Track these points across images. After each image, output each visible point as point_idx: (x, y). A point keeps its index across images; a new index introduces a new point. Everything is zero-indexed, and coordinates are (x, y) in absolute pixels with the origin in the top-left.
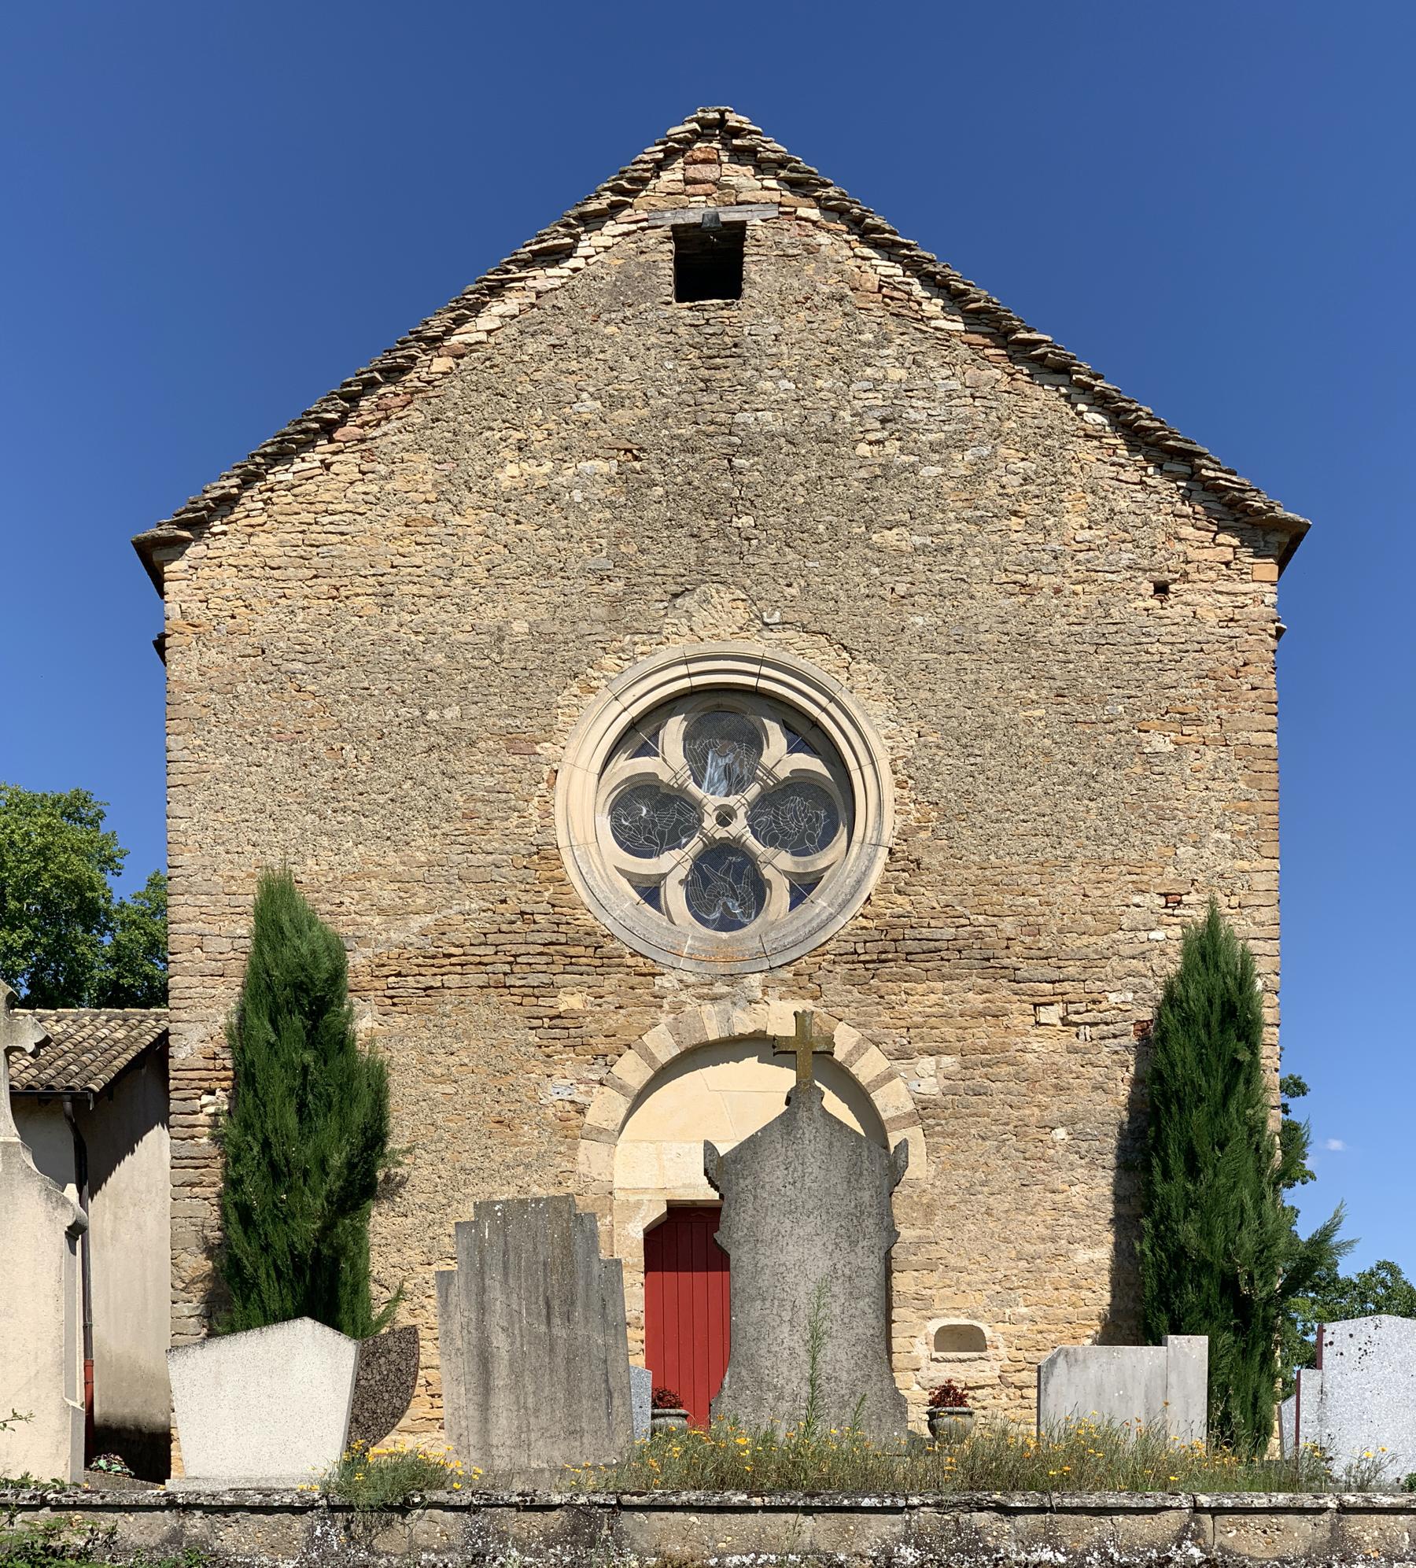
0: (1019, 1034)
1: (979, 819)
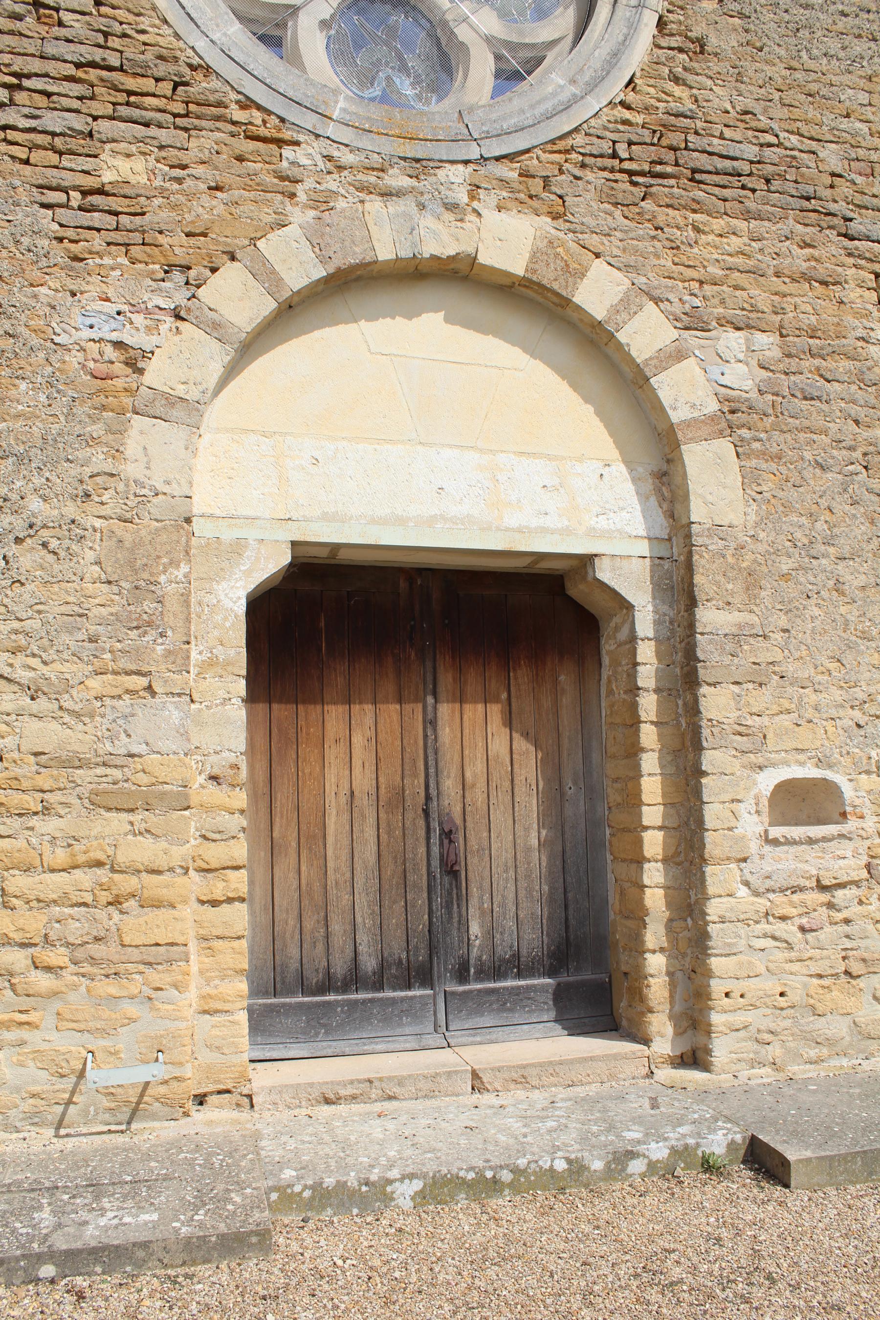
0: (858, 315)
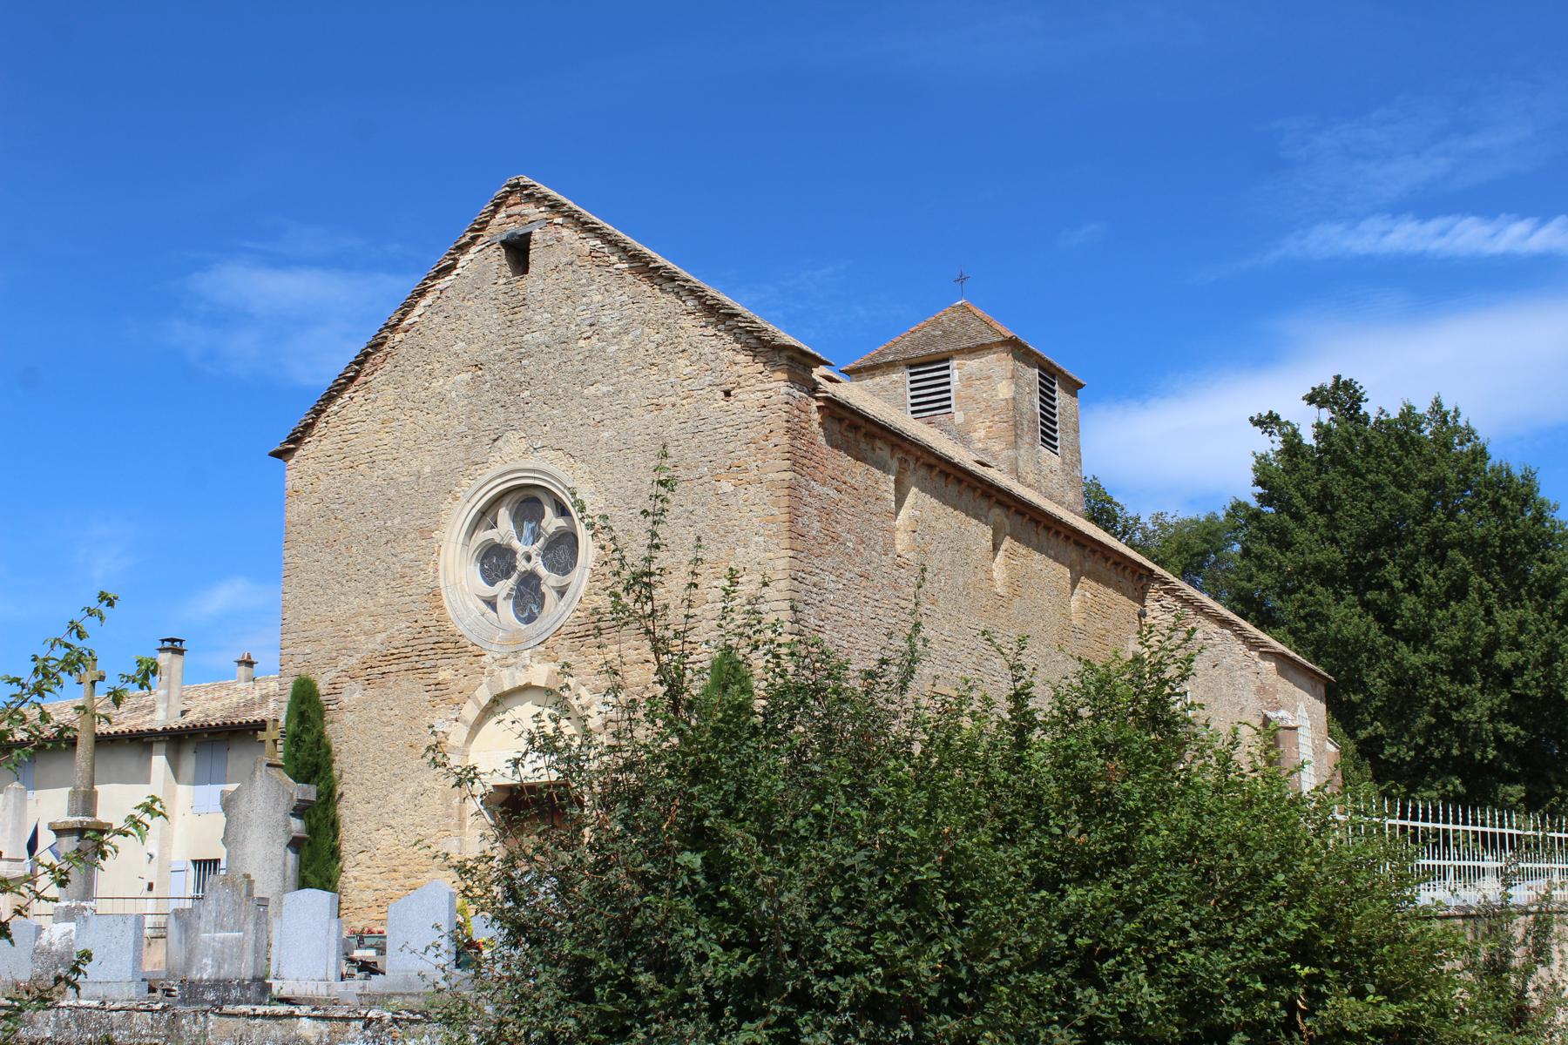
1: (634, 545)
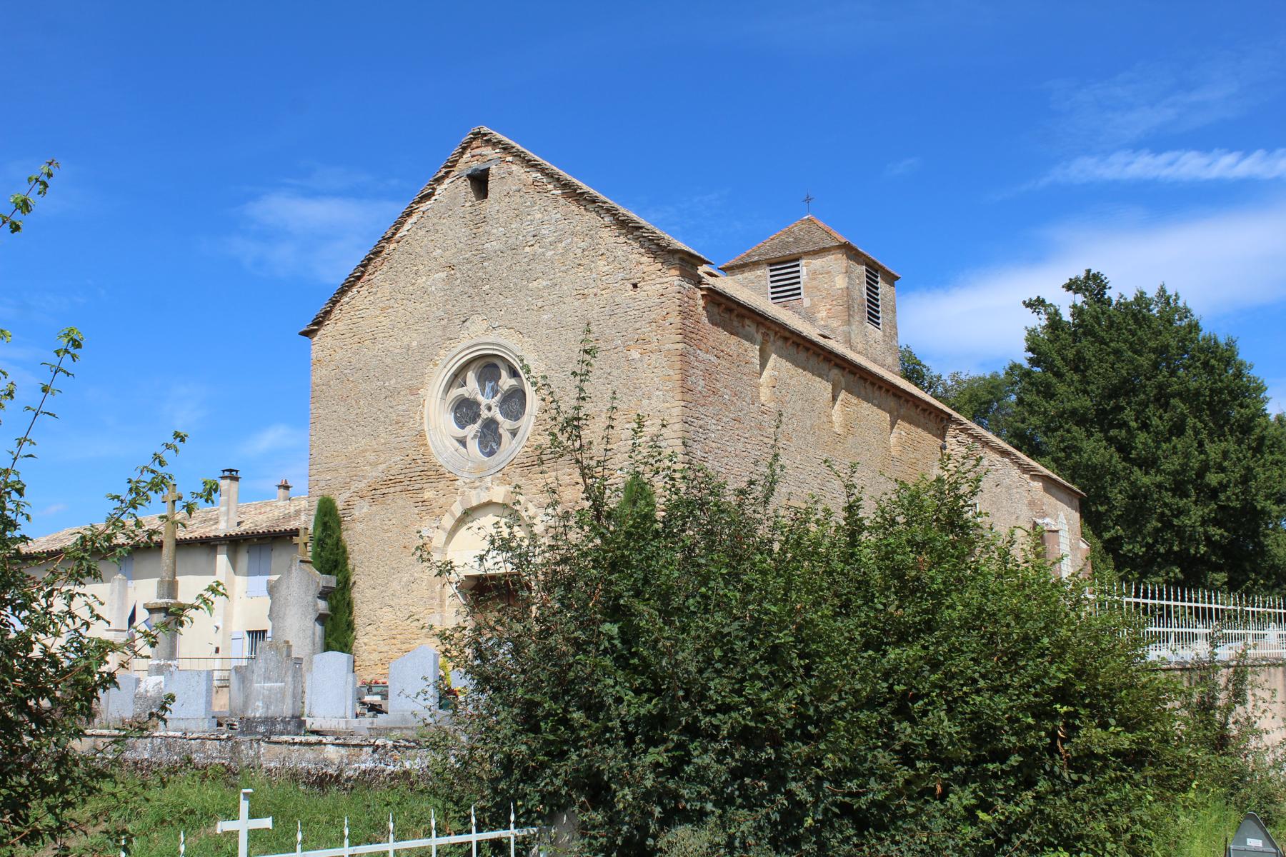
1: (567, 399)
